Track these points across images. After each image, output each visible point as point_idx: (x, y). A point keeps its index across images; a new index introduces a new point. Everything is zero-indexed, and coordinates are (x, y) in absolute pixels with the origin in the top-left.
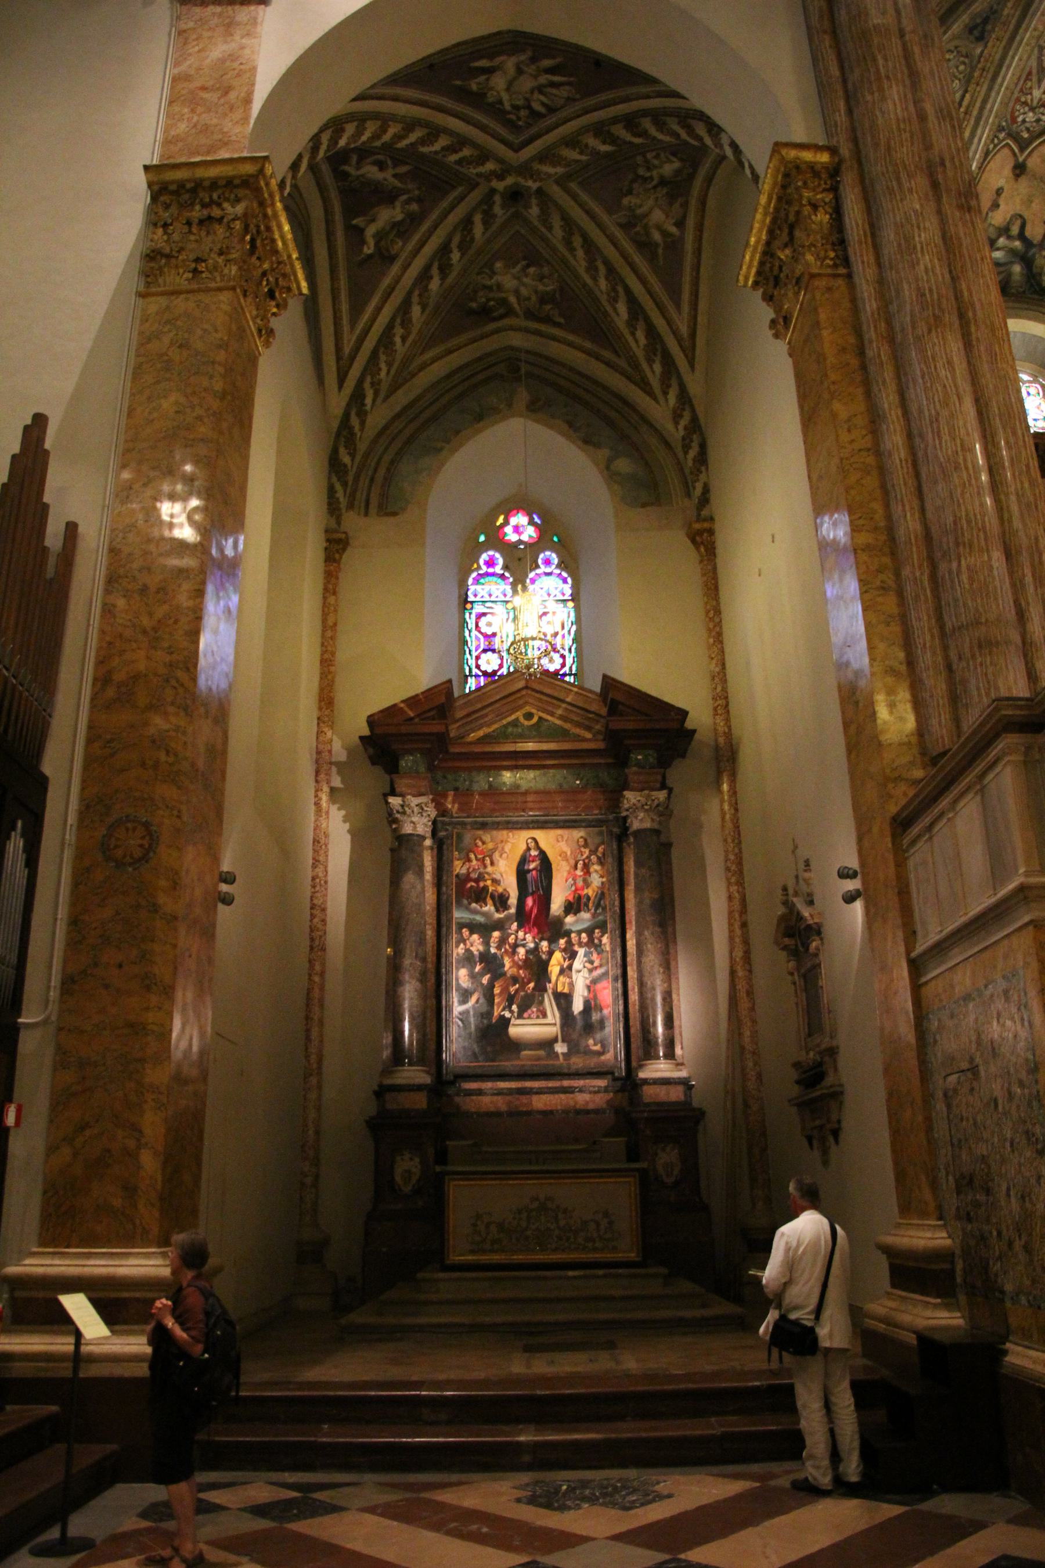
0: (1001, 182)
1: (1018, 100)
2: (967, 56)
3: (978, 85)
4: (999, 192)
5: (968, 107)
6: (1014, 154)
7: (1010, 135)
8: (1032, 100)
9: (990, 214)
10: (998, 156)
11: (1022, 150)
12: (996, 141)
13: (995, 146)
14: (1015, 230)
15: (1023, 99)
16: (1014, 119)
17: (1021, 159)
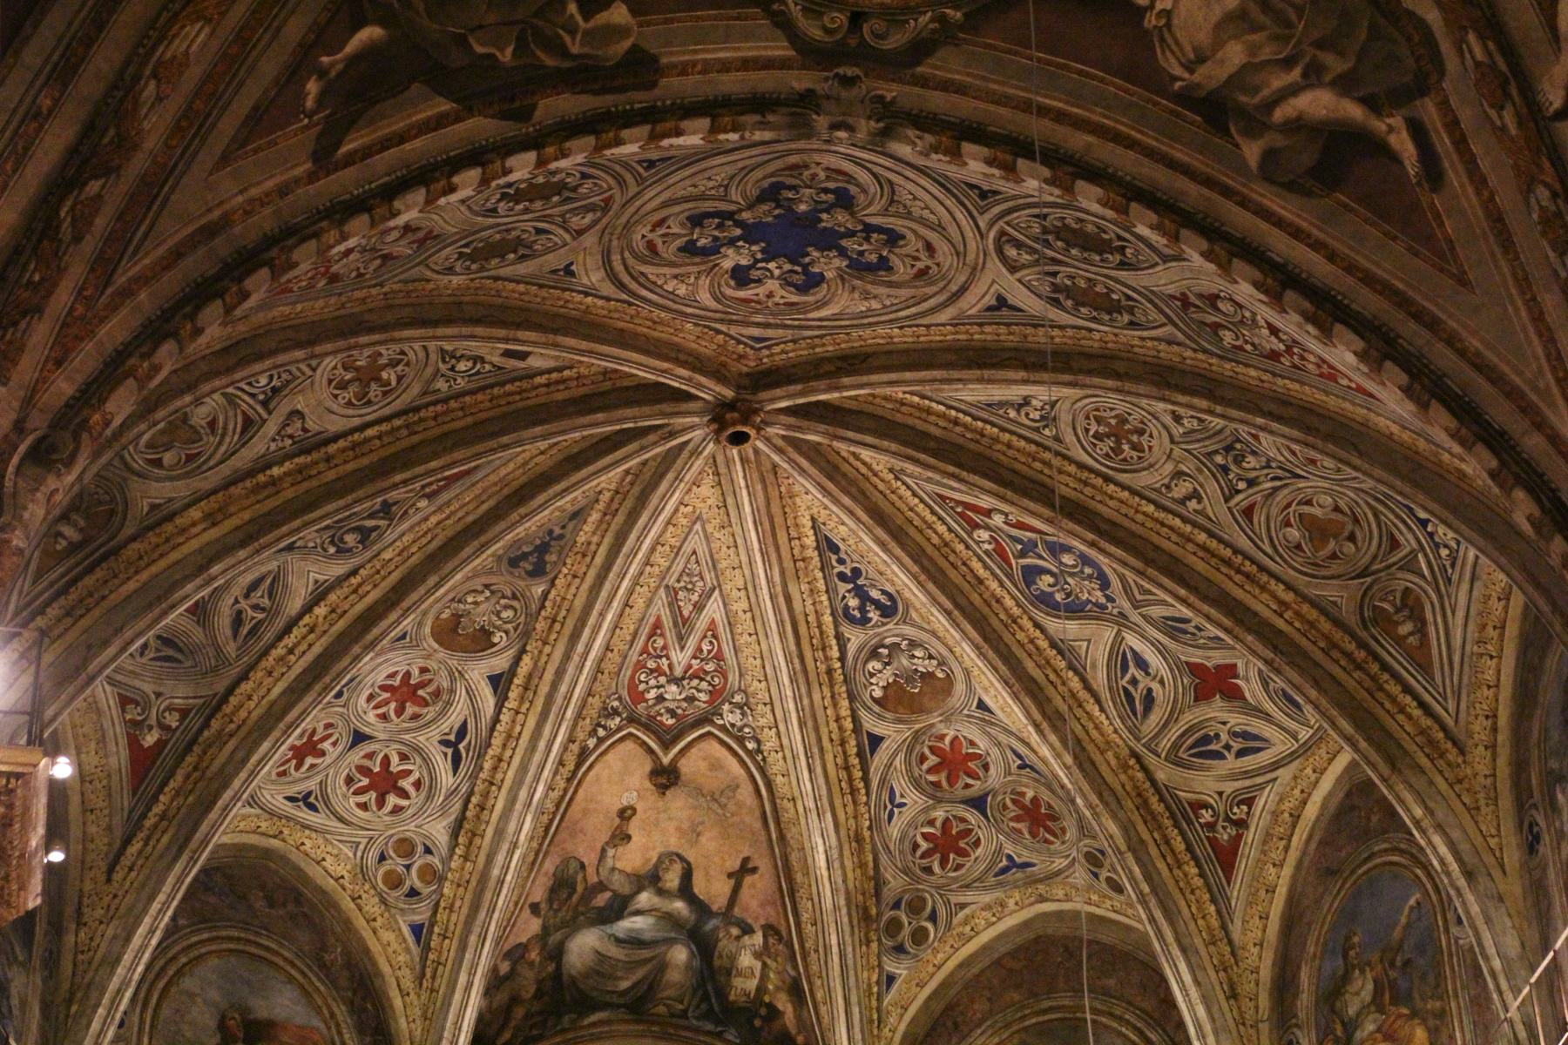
0: (628, 798)
1: (640, 666)
2: (514, 597)
3: (545, 643)
4: (626, 814)
5: (530, 677)
6: (650, 751)
7: (632, 720)
8: (670, 666)
9: (611, 852)
10: (610, 757)
11: (666, 746)
12: (601, 732)
13: (601, 741)
14: (672, 879)
15: (651, 664)
16: (639, 697)
17: (666, 760)
